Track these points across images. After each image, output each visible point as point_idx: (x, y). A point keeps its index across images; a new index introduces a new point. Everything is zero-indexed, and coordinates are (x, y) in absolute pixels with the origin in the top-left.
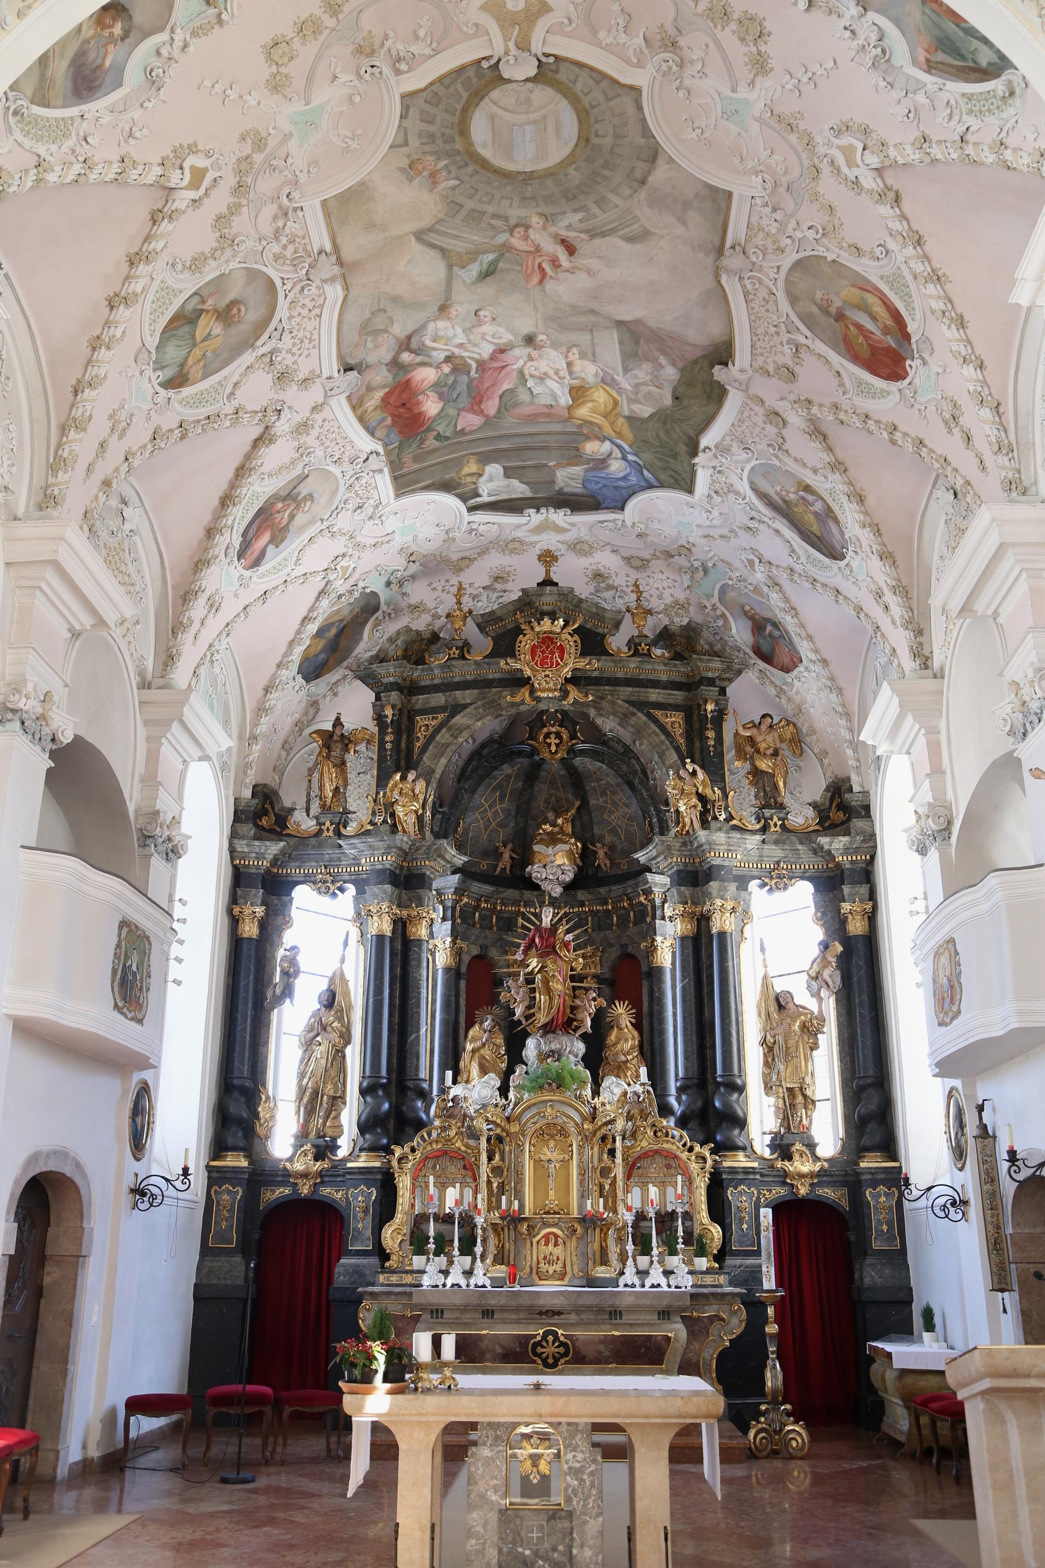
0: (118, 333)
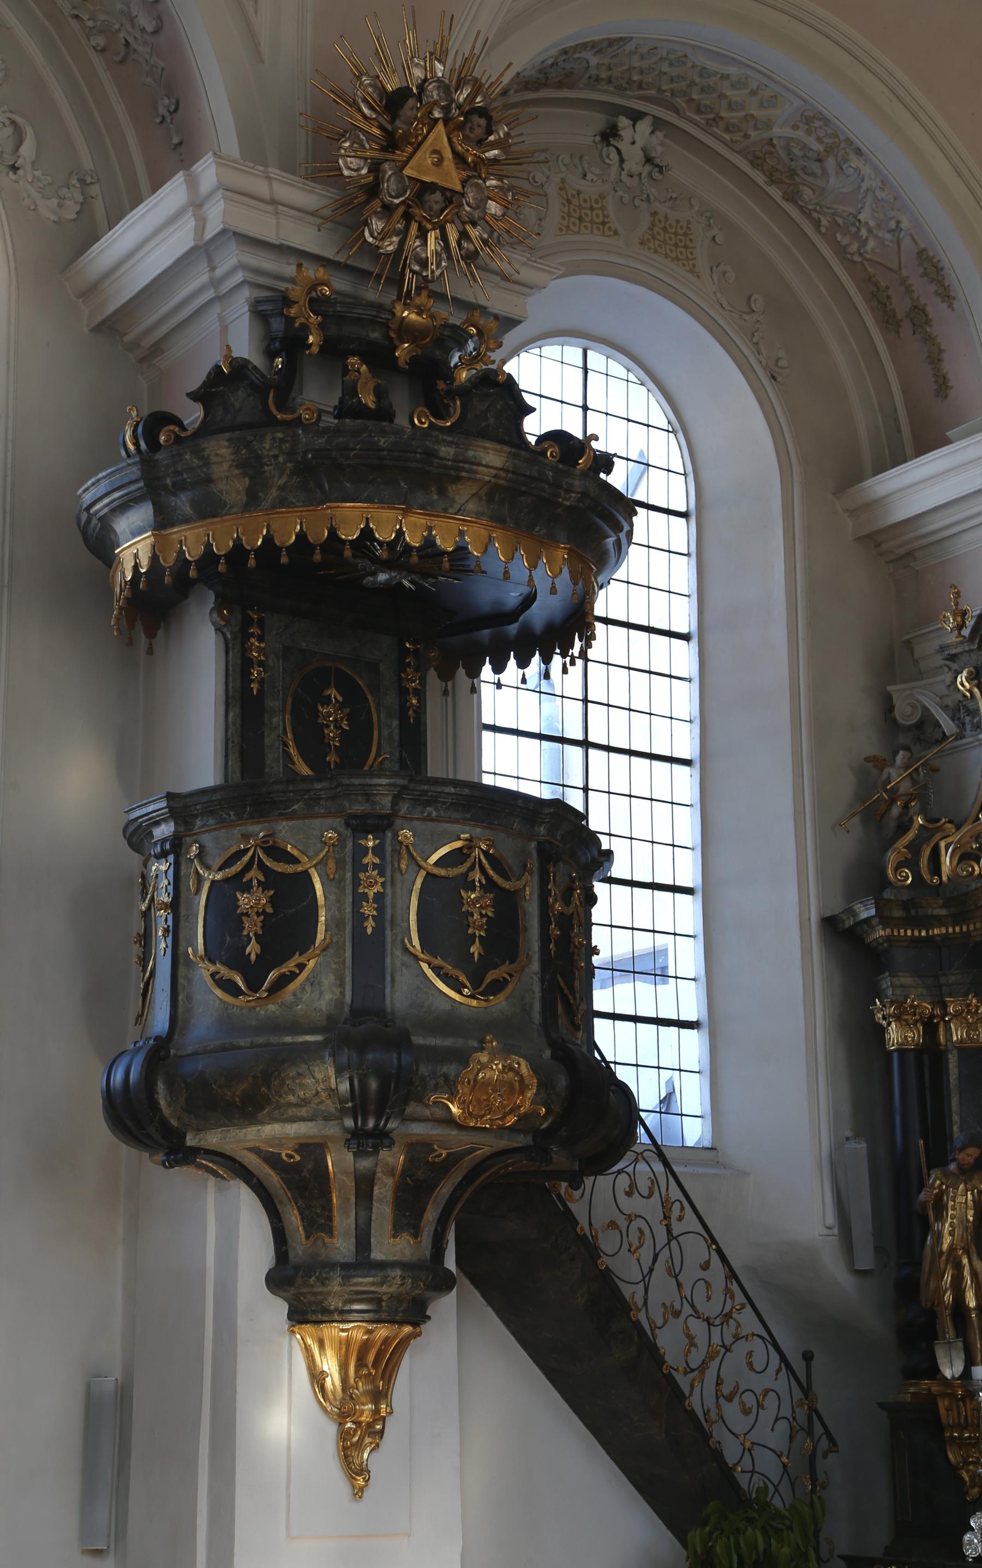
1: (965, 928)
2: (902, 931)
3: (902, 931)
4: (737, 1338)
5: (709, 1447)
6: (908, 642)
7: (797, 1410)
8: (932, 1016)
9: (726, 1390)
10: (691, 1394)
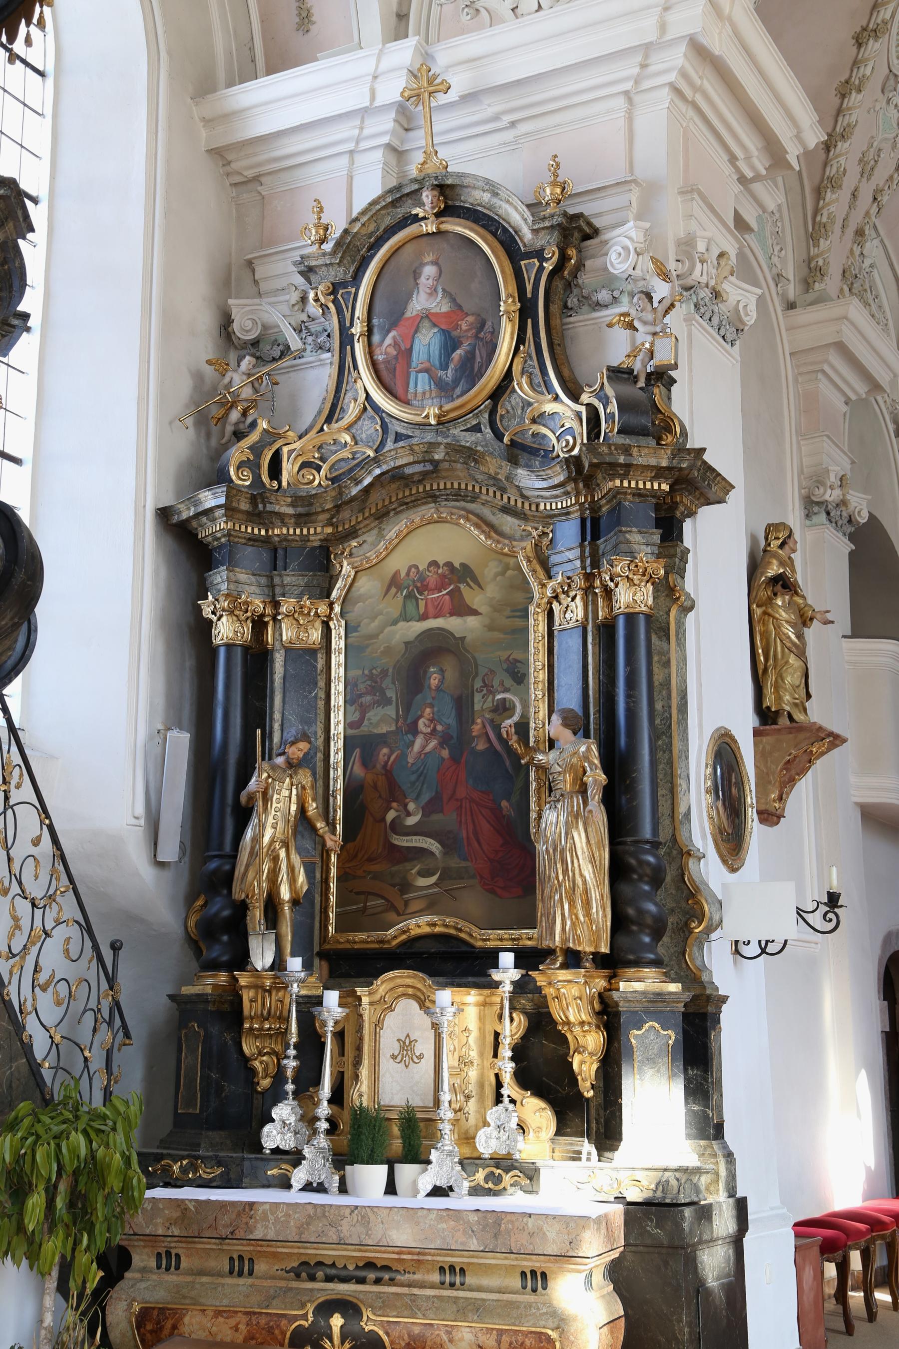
0: (868, 72)
1: (305, 531)
2: (243, 527)
3: (243, 527)
4: (58, 923)
5: (21, 1040)
6: (250, 263)
7: (103, 1001)
8: (263, 615)
9: (43, 978)
10: (10, 983)
